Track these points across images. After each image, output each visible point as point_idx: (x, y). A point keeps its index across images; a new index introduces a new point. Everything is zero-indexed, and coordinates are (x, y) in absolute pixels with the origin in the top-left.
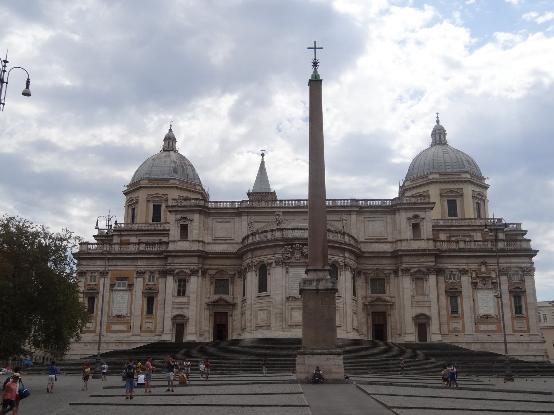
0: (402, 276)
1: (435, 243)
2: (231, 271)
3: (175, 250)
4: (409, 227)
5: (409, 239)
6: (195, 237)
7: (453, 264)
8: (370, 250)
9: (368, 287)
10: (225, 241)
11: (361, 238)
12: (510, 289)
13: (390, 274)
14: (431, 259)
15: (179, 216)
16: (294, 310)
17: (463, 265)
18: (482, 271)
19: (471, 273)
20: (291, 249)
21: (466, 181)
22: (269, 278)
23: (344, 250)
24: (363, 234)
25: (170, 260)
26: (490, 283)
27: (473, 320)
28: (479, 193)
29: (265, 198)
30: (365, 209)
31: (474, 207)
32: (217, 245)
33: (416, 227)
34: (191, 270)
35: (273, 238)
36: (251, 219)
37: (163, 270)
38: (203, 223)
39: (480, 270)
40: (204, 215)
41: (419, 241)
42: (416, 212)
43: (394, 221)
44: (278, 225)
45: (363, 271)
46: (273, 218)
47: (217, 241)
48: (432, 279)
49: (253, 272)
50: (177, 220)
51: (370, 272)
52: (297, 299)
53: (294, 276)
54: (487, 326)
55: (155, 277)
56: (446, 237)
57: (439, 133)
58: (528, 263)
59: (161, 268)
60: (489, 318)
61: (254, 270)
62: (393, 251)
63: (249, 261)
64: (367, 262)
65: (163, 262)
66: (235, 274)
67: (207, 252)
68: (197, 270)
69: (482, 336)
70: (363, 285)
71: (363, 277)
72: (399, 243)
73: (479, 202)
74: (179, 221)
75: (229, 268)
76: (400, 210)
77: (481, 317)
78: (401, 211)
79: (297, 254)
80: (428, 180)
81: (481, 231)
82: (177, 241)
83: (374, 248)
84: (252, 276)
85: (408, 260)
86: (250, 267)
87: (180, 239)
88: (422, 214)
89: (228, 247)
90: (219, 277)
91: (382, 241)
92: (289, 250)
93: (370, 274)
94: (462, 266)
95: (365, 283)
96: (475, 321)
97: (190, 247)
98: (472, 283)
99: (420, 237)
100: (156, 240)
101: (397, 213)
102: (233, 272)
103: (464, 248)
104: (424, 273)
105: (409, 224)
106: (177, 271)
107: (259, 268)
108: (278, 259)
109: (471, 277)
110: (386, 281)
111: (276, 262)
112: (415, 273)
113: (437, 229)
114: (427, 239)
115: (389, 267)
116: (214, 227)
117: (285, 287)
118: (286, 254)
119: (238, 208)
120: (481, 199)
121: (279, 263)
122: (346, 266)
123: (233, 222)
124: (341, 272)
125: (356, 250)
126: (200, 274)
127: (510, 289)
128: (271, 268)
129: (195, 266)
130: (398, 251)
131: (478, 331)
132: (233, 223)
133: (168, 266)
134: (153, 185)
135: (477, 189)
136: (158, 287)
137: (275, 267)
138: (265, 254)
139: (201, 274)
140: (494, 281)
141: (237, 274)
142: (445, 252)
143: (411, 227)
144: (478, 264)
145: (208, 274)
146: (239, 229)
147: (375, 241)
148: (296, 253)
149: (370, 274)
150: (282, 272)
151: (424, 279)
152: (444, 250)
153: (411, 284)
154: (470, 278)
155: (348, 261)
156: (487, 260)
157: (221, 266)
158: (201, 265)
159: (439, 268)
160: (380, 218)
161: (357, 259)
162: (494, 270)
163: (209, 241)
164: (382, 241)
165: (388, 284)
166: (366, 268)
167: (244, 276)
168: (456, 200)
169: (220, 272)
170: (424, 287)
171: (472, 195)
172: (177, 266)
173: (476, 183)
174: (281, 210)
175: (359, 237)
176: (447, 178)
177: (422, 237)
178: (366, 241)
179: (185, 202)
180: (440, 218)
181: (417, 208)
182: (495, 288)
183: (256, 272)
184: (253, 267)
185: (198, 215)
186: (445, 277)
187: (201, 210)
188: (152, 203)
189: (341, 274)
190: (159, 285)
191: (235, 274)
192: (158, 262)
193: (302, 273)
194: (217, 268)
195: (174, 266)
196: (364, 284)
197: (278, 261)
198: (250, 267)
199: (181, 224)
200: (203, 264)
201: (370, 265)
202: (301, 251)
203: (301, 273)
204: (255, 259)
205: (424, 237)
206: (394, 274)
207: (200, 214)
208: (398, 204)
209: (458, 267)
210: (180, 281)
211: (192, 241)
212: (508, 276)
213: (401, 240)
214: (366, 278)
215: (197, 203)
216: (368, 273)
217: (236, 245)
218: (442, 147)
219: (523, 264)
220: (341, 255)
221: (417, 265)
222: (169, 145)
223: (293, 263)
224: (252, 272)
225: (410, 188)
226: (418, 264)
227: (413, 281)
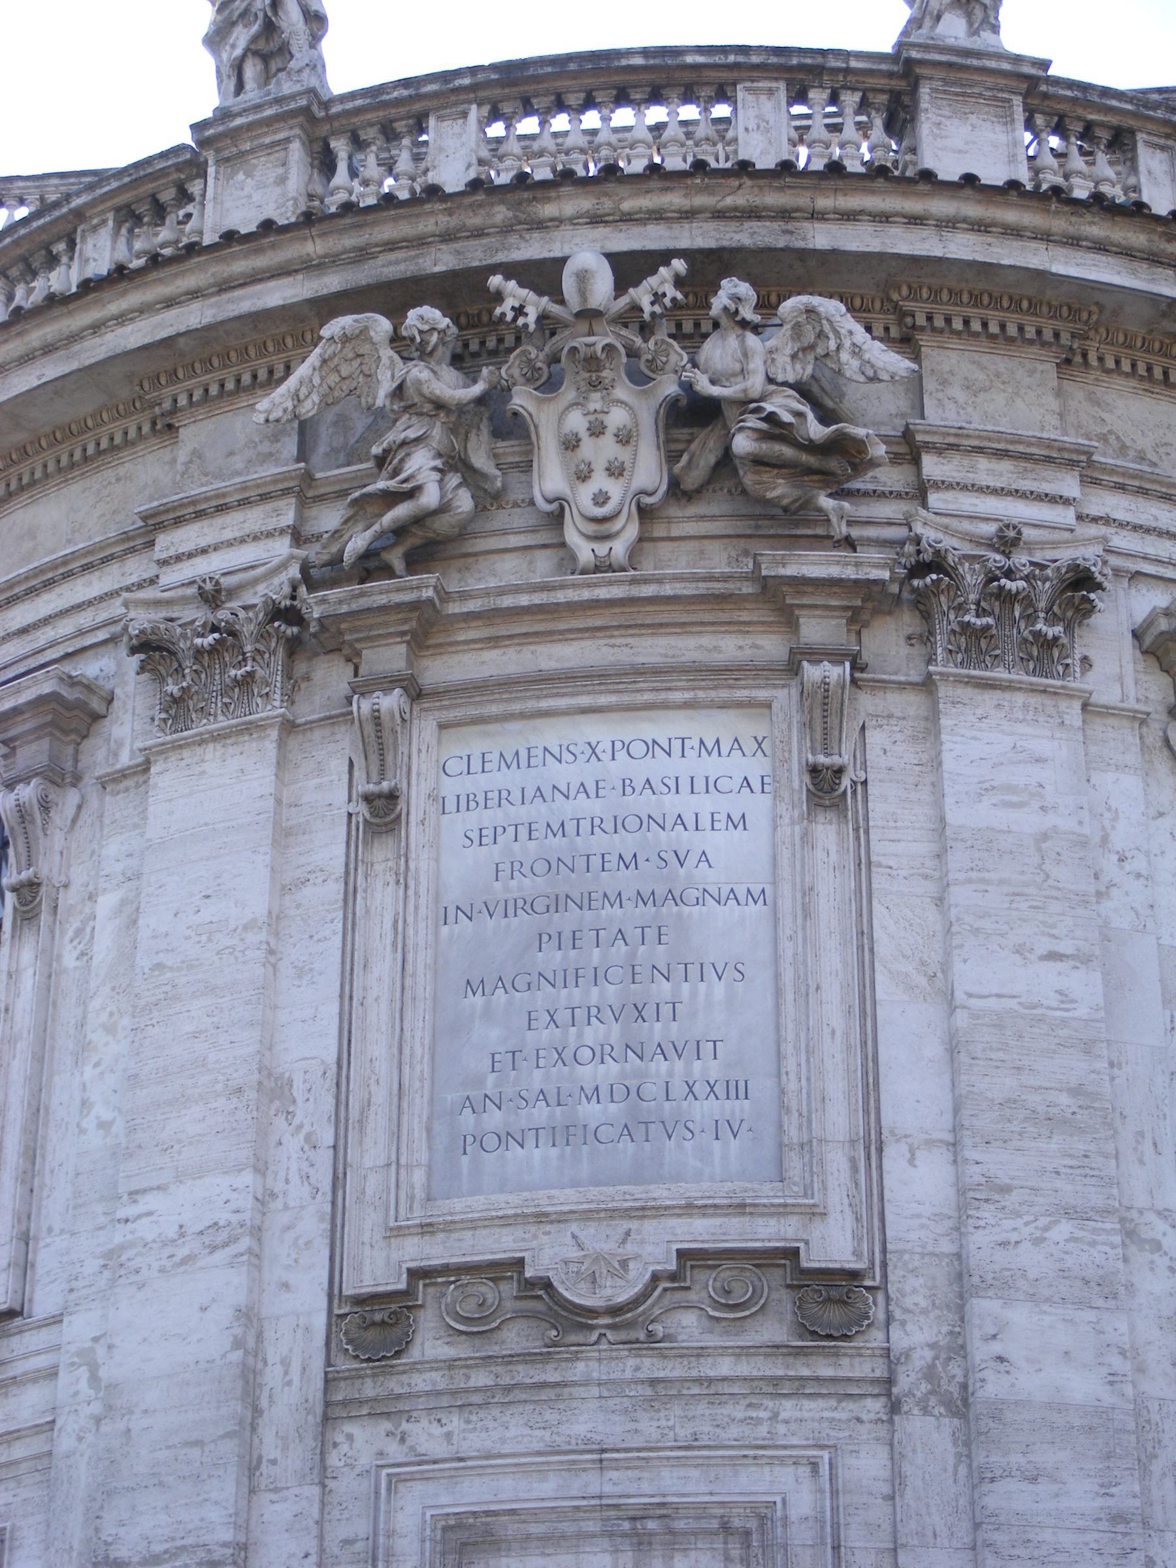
79: (588, 449)
128: (72, 798)
148: (570, 444)
193: (705, 804)
203: (672, 804)
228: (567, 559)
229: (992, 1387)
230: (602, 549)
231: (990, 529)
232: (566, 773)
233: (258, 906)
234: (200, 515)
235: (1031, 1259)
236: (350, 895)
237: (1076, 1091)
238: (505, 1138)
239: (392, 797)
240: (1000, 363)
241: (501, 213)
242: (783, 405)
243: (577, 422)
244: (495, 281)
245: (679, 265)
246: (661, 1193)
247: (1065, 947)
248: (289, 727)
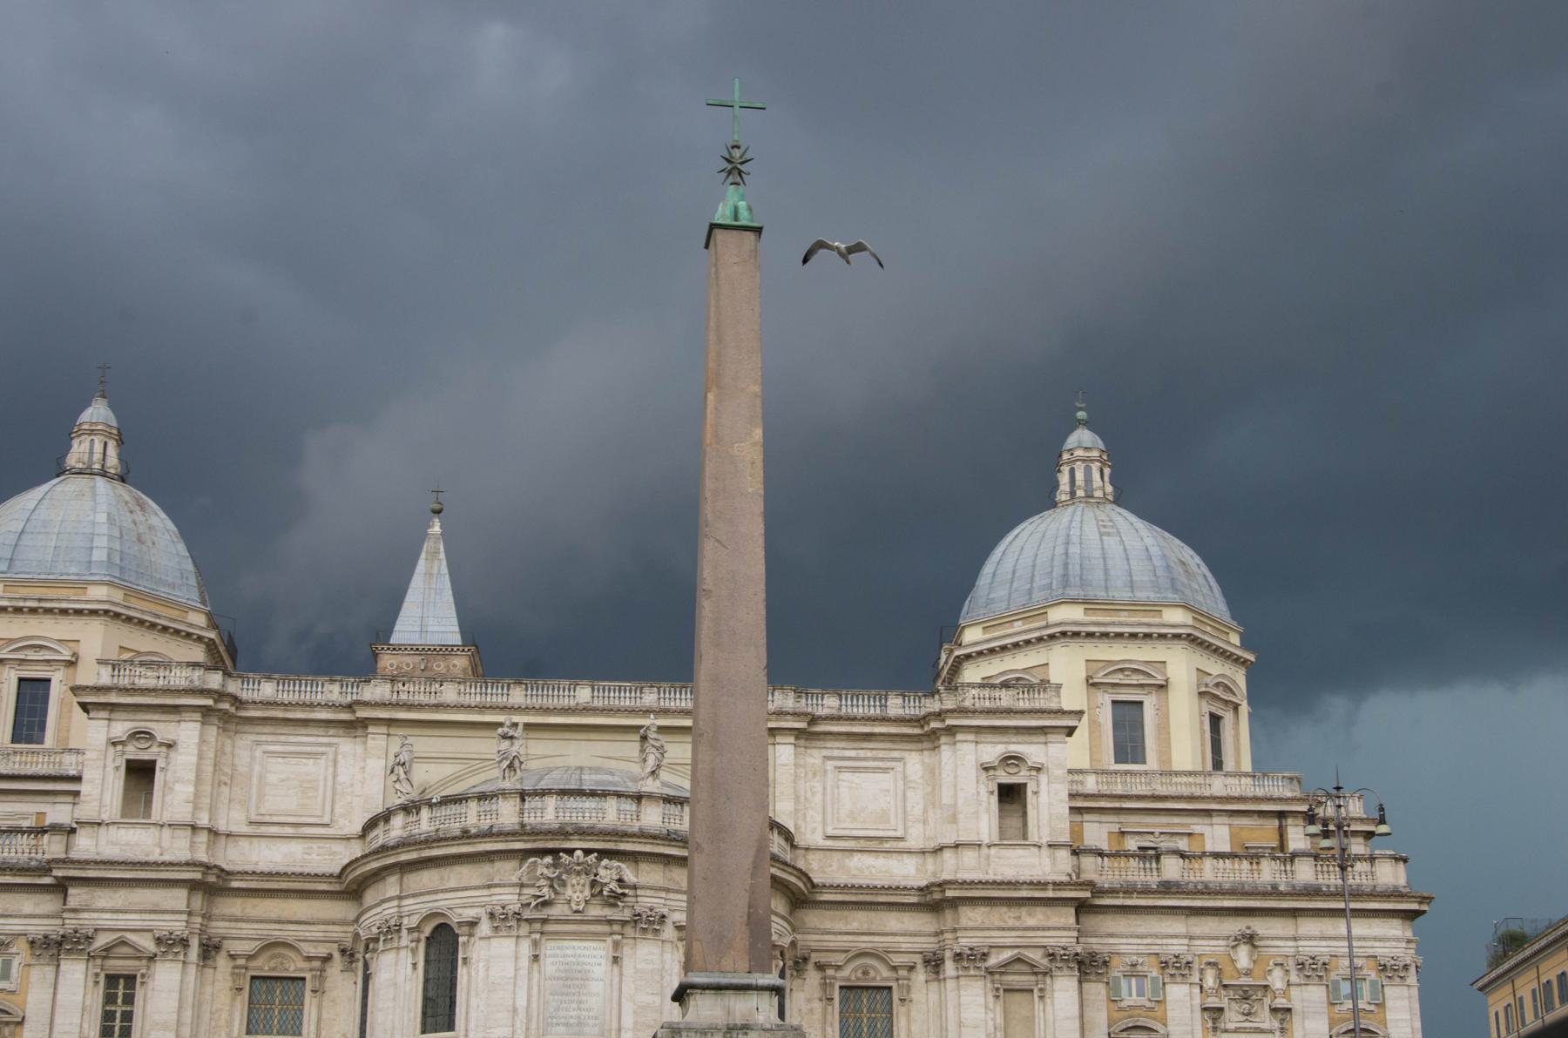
0: (958, 977)
1: (1075, 858)
2: (315, 947)
3: (99, 858)
4: (985, 799)
5: (986, 841)
6: (182, 813)
7: (1138, 937)
8: (842, 879)
9: (829, 1017)
10: (297, 830)
11: (811, 835)
12: (1333, 1032)
13: (911, 968)
14: (1062, 920)
15: (121, 728)
17: (1175, 941)
18: (1239, 966)
19: (1202, 971)
20: (552, 869)
21: (1177, 637)
22: (465, 978)
24: (819, 818)
25: (76, 895)
26: (1267, 1008)
28: (1220, 680)
29: (438, 666)
30: (826, 724)
31: (1203, 732)
32: (264, 842)
33: (1011, 795)
34: (158, 939)
35: (485, 824)
36: (405, 748)
37: (46, 937)
38: (212, 756)
39: (1233, 961)
40: (219, 728)
41: (1020, 852)
42: (1014, 743)
43: (932, 773)
44: (507, 775)
45: (813, 955)
46: (487, 746)
47: (264, 830)
48: (1064, 990)
49: (403, 953)
50: (114, 744)
51: (839, 959)
53: (564, 975)
55: (15, 964)
56: (1105, 836)
57: (1084, 461)
58: (1397, 939)
59: (40, 928)
61: (407, 947)
62: (927, 887)
63: (390, 910)
64: (828, 925)
65: (48, 903)
66: (328, 959)
67: (222, 870)
68: (183, 939)
70: (811, 1010)
71: (813, 977)
72: (947, 854)
73: (1220, 713)
74: (119, 748)
75: (307, 934)
76: (954, 735)
78: (959, 737)
79: (576, 887)
80: (1047, 627)
81: (1230, 816)
82: (107, 824)
83: (855, 872)
84: (396, 970)
85: (980, 921)
86: (392, 930)
87: (122, 817)
88: (1032, 751)
89: (307, 853)
90: (266, 968)
91: (887, 846)
92: (545, 871)
93: (838, 968)
94: (1170, 947)
95: (821, 1000)
97: (161, 847)
98: (1205, 1009)
99: (1025, 837)
100: (24, 817)
101: (945, 744)
102: (322, 951)
103: (1180, 879)
104: (1036, 970)
105: (987, 786)
106: (102, 940)
107: (428, 938)
108: (503, 908)
109: (1201, 987)
110: (896, 996)
111: (492, 915)
112: (1003, 970)
113: (1079, 807)
114: (1050, 846)
115: (909, 945)
116: (255, 780)
117: (522, 1014)
118: (533, 886)
119: (350, 707)
120: (1226, 702)
121: (502, 920)
123: (331, 757)
125: (793, 879)
126: (194, 952)
127: (1333, 1032)
128: (472, 940)
129: (177, 925)
130: (942, 885)
132: (330, 763)
133: (67, 921)
134: (21, 604)
135: (1216, 668)
136: (25, 1002)
137: (489, 938)
138: (452, 884)
139: (199, 955)
140: (1281, 1002)
141: (337, 955)
142: (1112, 892)
143: (995, 798)
144: (1228, 938)
145: (223, 953)
146: (352, 785)
147: (862, 844)
148: (573, 886)
149: (838, 968)
150: (516, 958)
151: (1036, 991)
152: (1106, 886)
153: (986, 1007)
154: (1198, 990)
156: (1260, 926)
157: (277, 926)
158: (199, 920)
159: (1089, 953)
160: (882, 759)
161: (791, 913)
162: (1282, 965)
163: (234, 829)
165: (903, 1010)
166: (825, 944)
167: (366, 966)
168: (1141, 703)
169: (271, 945)
170: (1034, 1022)
171: (1198, 687)
172: (105, 920)
173: (1210, 645)
174: (521, 719)
175: (803, 830)
176: (1113, 624)
177: (1033, 836)
178: (829, 843)
179: (149, 674)
180: (1085, 765)
181: (1019, 730)
182: (1282, 1030)
183: (414, 951)
184: (404, 932)
185: (198, 725)
186: (1107, 983)
187: (211, 706)
188: (13, 673)
190: (29, 998)
191: (328, 959)
192: (28, 904)
194: (259, 932)
195: (93, 922)
196: (817, 1005)
197: (503, 914)
198: (392, 930)
199: (128, 762)
200: (207, 917)
201: (840, 933)
202: (593, 878)
203: (588, 960)
204: (411, 901)
205: (1040, 838)
206: (926, 972)
207: (203, 723)
208: (948, 711)
209: (1156, 949)
210: (112, 980)
211: (170, 825)
212: (1327, 986)
213: (957, 846)
214: (825, 984)
215: (195, 678)
216: (830, 966)
217: (337, 847)
218: (1096, 510)
219: (1381, 944)
221: (1012, 940)
222: (91, 453)
223: (558, 921)
224: (398, 954)
225: (980, 653)
226: (1013, 934)
227: (997, 997)
228: (571, 908)
230: (578, 907)
231: (649, 905)
232: (569, 952)
233: (512, 975)
234: (500, 887)
236: (530, 973)
237: (654, 1020)
238: (557, 1024)
239: (537, 956)
240: (653, 866)
241: (563, 837)
242: (613, 886)
243: (574, 882)
244: (561, 854)
245: (596, 854)
247: (655, 992)
248: (518, 937)
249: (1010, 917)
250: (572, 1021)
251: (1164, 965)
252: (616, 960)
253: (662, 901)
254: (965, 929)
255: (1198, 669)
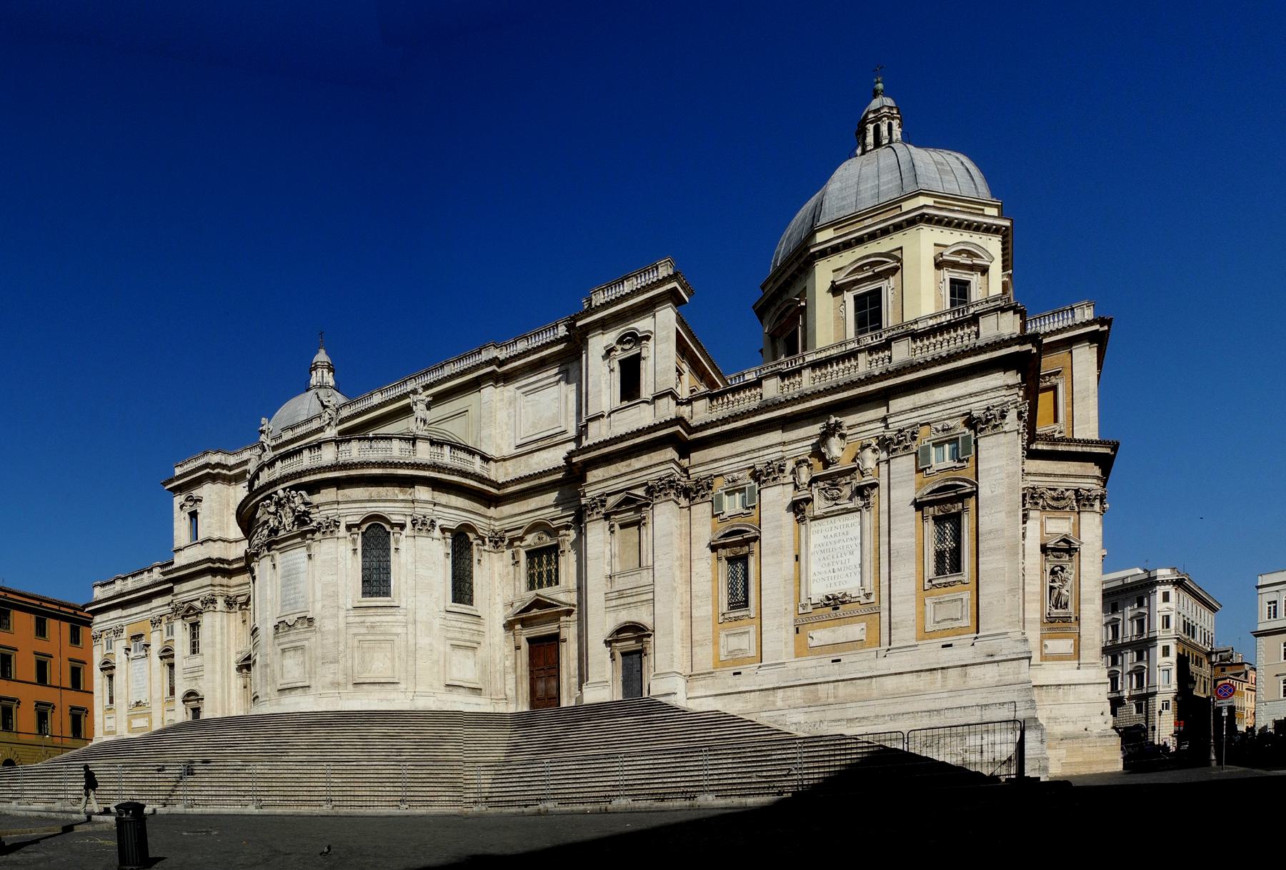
16: (287, 654)
23: (407, 482)
27: (790, 619)
52: (290, 626)
54: (833, 631)
60: (841, 607)
69: (814, 663)
77: (815, 606)
85: (601, 476)
96: (795, 620)
122: (424, 525)
124: (397, 541)
131: (803, 650)
155: (420, 511)
164: (555, 440)
186: (712, 501)
189: (397, 549)
203: (298, 561)
220: (401, 497)
221: (623, 484)
229: (323, 629)
232: (289, 558)
235: (327, 614)
238: (286, 605)
245: (288, 489)
246: (297, 611)
249: (622, 467)
250: (292, 601)
251: (756, 476)
252: (310, 556)
253: (336, 511)
254: (590, 485)
255: (935, 245)
